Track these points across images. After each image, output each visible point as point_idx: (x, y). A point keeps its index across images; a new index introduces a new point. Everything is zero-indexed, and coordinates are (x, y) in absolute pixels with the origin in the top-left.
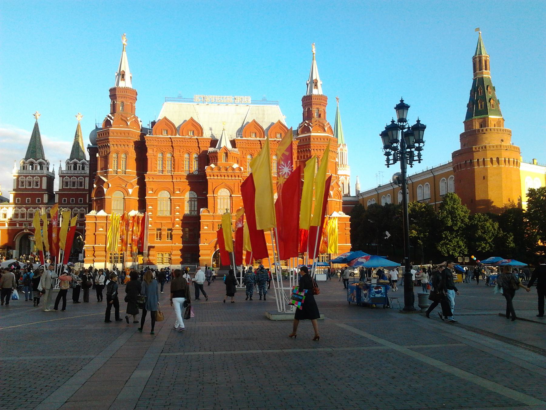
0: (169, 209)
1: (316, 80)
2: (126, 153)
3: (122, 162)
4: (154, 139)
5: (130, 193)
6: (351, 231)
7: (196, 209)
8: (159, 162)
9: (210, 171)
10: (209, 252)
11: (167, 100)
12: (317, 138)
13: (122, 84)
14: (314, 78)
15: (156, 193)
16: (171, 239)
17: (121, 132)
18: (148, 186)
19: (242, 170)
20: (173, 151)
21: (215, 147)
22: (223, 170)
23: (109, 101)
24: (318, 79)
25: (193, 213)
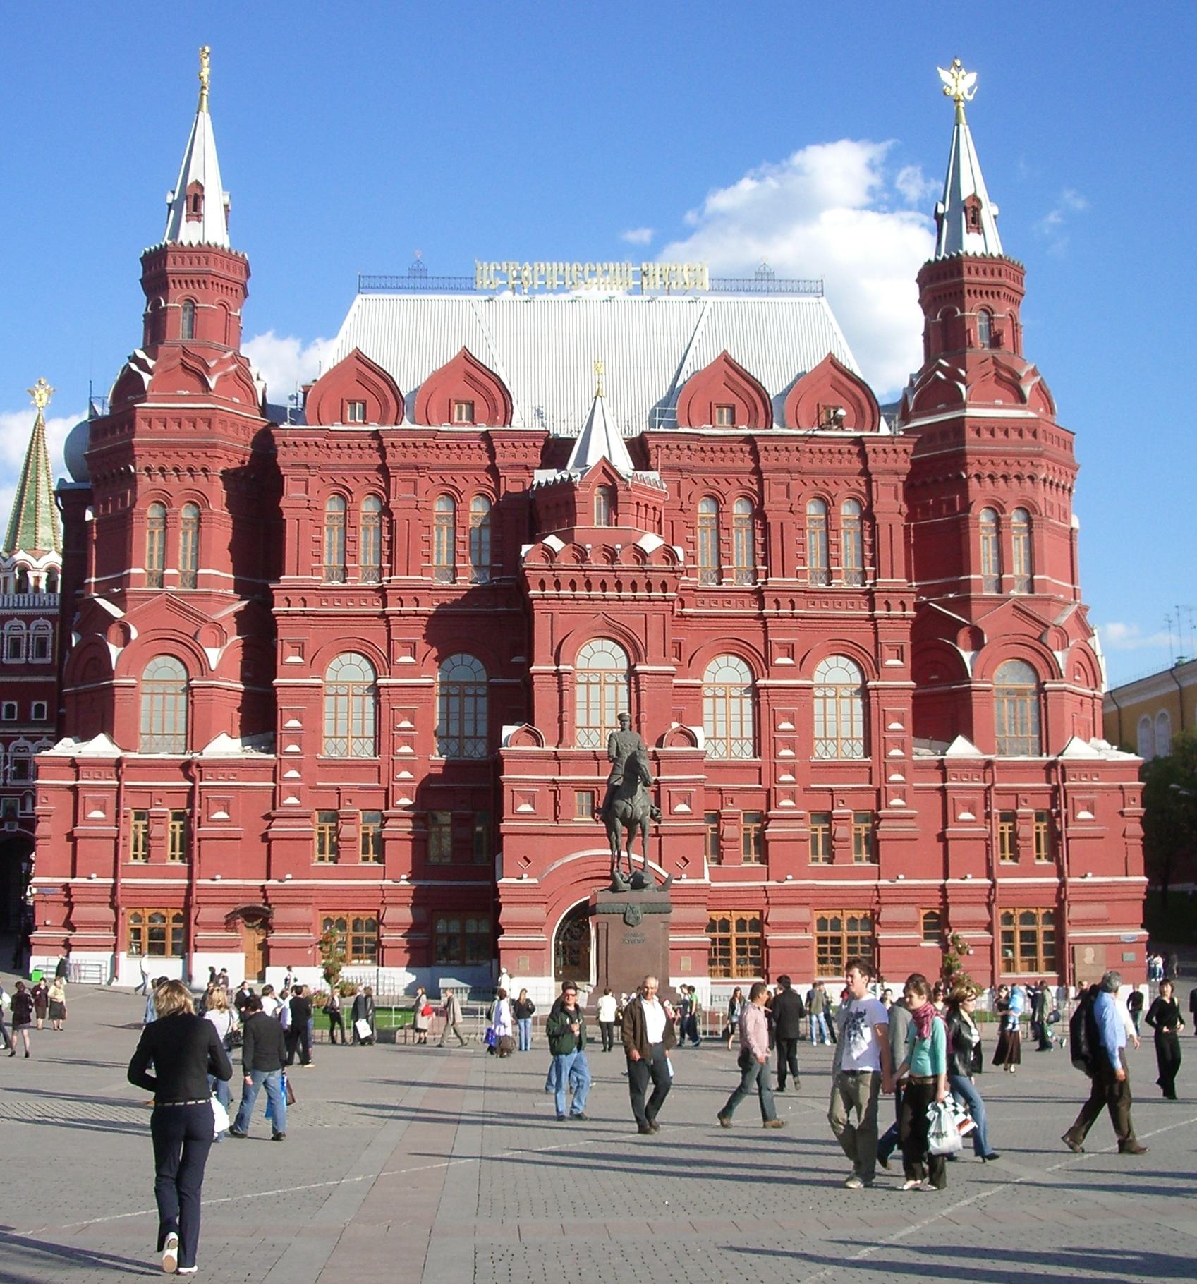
0: (370, 731)
1: (974, 198)
2: (200, 501)
3: (184, 542)
4: (310, 440)
5: (213, 666)
6: (1144, 822)
7: (483, 729)
8: (331, 538)
9: (543, 564)
10: (538, 913)
11: (370, 284)
12: (993, 427)
13: (190, 234)
14: (966, 193)
15: (315, 662)
16: (380, 858)
17: (179, 418)
18: (285, 635)
19: (681, 557)
20: (387, 491)
21: (561, 466)
22: (596, 560)
23: (139, 303)
24: (982, 194)
25: (469, 747)
